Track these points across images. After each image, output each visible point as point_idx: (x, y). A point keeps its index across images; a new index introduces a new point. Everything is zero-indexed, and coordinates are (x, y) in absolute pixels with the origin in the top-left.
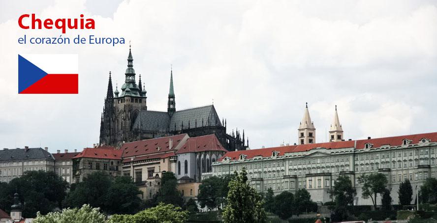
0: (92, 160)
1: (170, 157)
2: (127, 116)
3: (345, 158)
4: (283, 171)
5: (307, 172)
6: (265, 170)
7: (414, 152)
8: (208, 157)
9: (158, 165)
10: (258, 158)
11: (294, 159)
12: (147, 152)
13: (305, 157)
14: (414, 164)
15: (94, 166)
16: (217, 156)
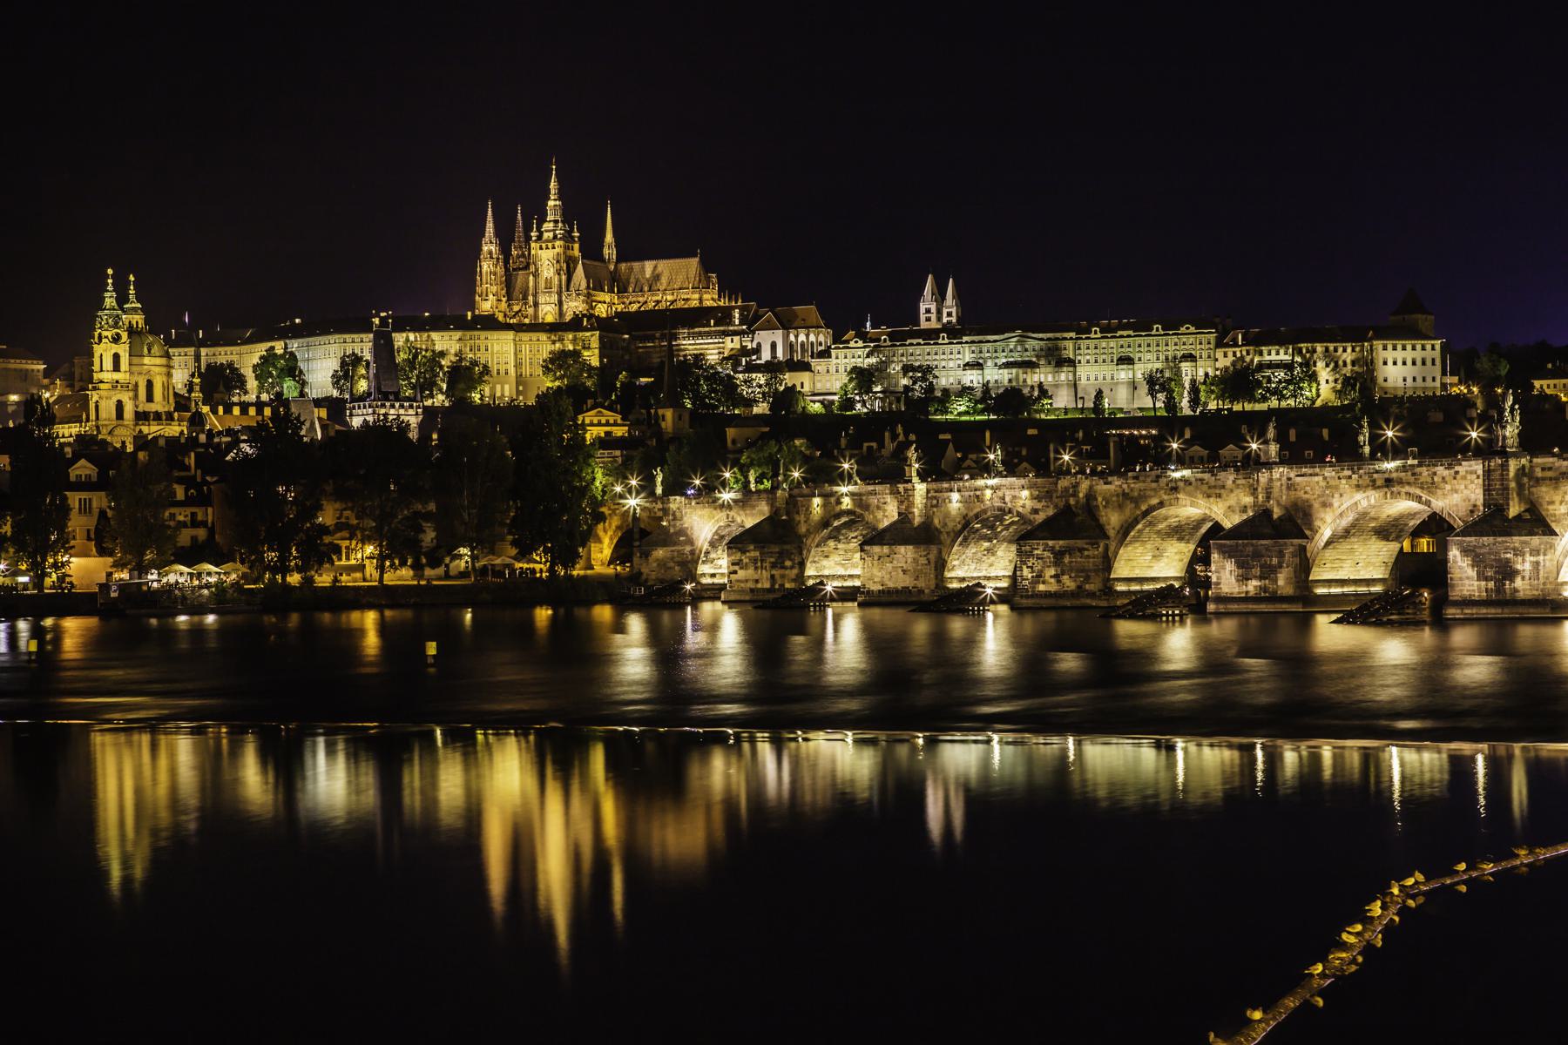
2: (561, 269)
8: (812, 338)
10: (914, 341)
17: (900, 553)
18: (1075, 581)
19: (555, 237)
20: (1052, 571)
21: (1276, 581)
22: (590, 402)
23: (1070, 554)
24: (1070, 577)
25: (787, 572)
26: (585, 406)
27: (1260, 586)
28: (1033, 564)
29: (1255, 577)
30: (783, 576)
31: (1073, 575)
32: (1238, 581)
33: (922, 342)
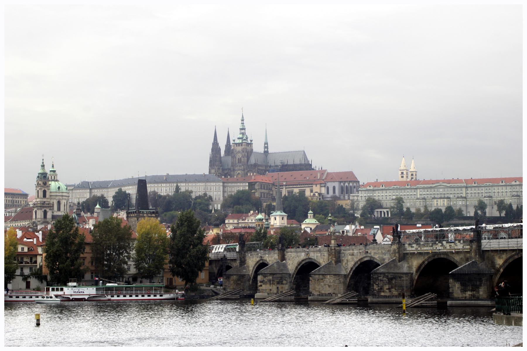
0: (262, 183)
1: (321, 184)
2: (245, 155)
3: (460, 189)
4: (415, 195)
5: (433, 196)
6: (401, 194)
7: (508, 188)
8: (351, 184)
9: (311, 188)
10: (395, 187)
11: (424, 188)
12: (295, 180)
13: (431, 188)
14: (509, 194)
15: (263, 187)
16: (357, 185)
17: (327, 278)
18: (398, 291)
19: (242, 141)
20: (387, 287)
21: (479, 292)
22: (252, 212)
23: (395, 279)
24: (395, 289)
25: (284, 286)
26: (249, 213)
27: (471, 294)
28: (379, 283)
29: (469, 290)
30: (282, 288)
31: (397, 288)
32: (461, 292)
33: (399, 187)
